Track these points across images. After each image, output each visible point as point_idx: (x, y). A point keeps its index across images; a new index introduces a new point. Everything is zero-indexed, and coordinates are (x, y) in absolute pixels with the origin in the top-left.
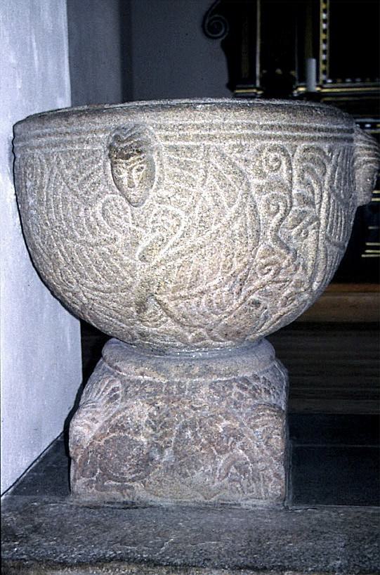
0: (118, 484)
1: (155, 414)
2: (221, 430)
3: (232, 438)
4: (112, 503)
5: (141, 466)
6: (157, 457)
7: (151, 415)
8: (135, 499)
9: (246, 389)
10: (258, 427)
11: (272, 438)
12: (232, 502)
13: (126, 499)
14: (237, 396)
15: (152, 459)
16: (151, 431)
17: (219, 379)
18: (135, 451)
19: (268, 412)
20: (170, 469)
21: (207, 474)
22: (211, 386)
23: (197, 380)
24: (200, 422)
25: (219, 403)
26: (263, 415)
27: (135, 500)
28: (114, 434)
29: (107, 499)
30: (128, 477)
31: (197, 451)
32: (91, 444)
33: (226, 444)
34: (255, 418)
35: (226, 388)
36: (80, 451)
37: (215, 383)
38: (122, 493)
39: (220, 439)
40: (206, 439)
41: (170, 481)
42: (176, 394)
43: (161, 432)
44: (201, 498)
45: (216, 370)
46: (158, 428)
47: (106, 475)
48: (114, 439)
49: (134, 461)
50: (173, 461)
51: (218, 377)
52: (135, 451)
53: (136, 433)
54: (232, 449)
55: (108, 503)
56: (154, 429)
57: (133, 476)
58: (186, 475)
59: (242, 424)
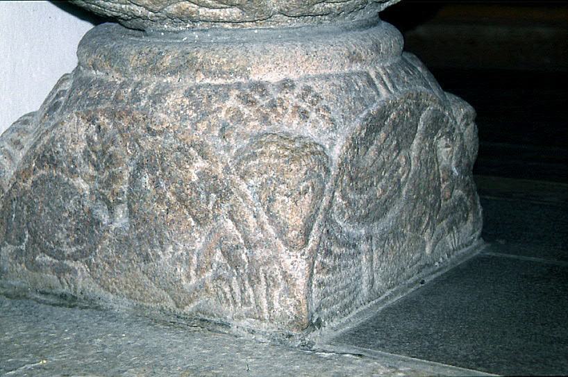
0: (54, 261)
1: (96, 138)
2: (195, 178)
3: (213, 195)
4: (46, 294)
5: (83, 232)
6: (105, 219)
7: (89, 140)
8: (79, 291)
9: (253, 103)
10: (252, 176)
11: (275, 201)
12: (217, 320)
13: (66, 289)
14: (231, 114)
15: (98, 223)
16: (91, 170)
17: (208, 81)
18: (71, 205)
19: (273, 148)
20: (123, 243)
21: (179, 259)
22: (188, 94)
23: (169, 79)
24: (162, 159)
25: (193, 125)
26: (262, 153)
27: (78, 295)
28: (42, 172)
29: (40, 286)
30: (68, 250)
31: (162, 215)
32: (14, 186)
33: (204, 206)
34: (248, 159)
35: (214, 99)
36: (451, 101)
37: (198, 87)
38: (59, 278)
39: (194, 194)
40: (174, 194)
41: (124, 266)
42: (128, 103)
43: (107, 173)
44: (171, 304)
45: (201, 64)
46: (102, 166)
47: (37, 244)
48: (43, 180)
49: (72, 222)
50: (127, 228)
51: (206, 76)
52: (71, 205)
53: (73, 173)
54: (215, 217)
55: (42, 293)
56: (96, 167)
57: (74, 249)
58: (147, 259)
59: (227, 169)
